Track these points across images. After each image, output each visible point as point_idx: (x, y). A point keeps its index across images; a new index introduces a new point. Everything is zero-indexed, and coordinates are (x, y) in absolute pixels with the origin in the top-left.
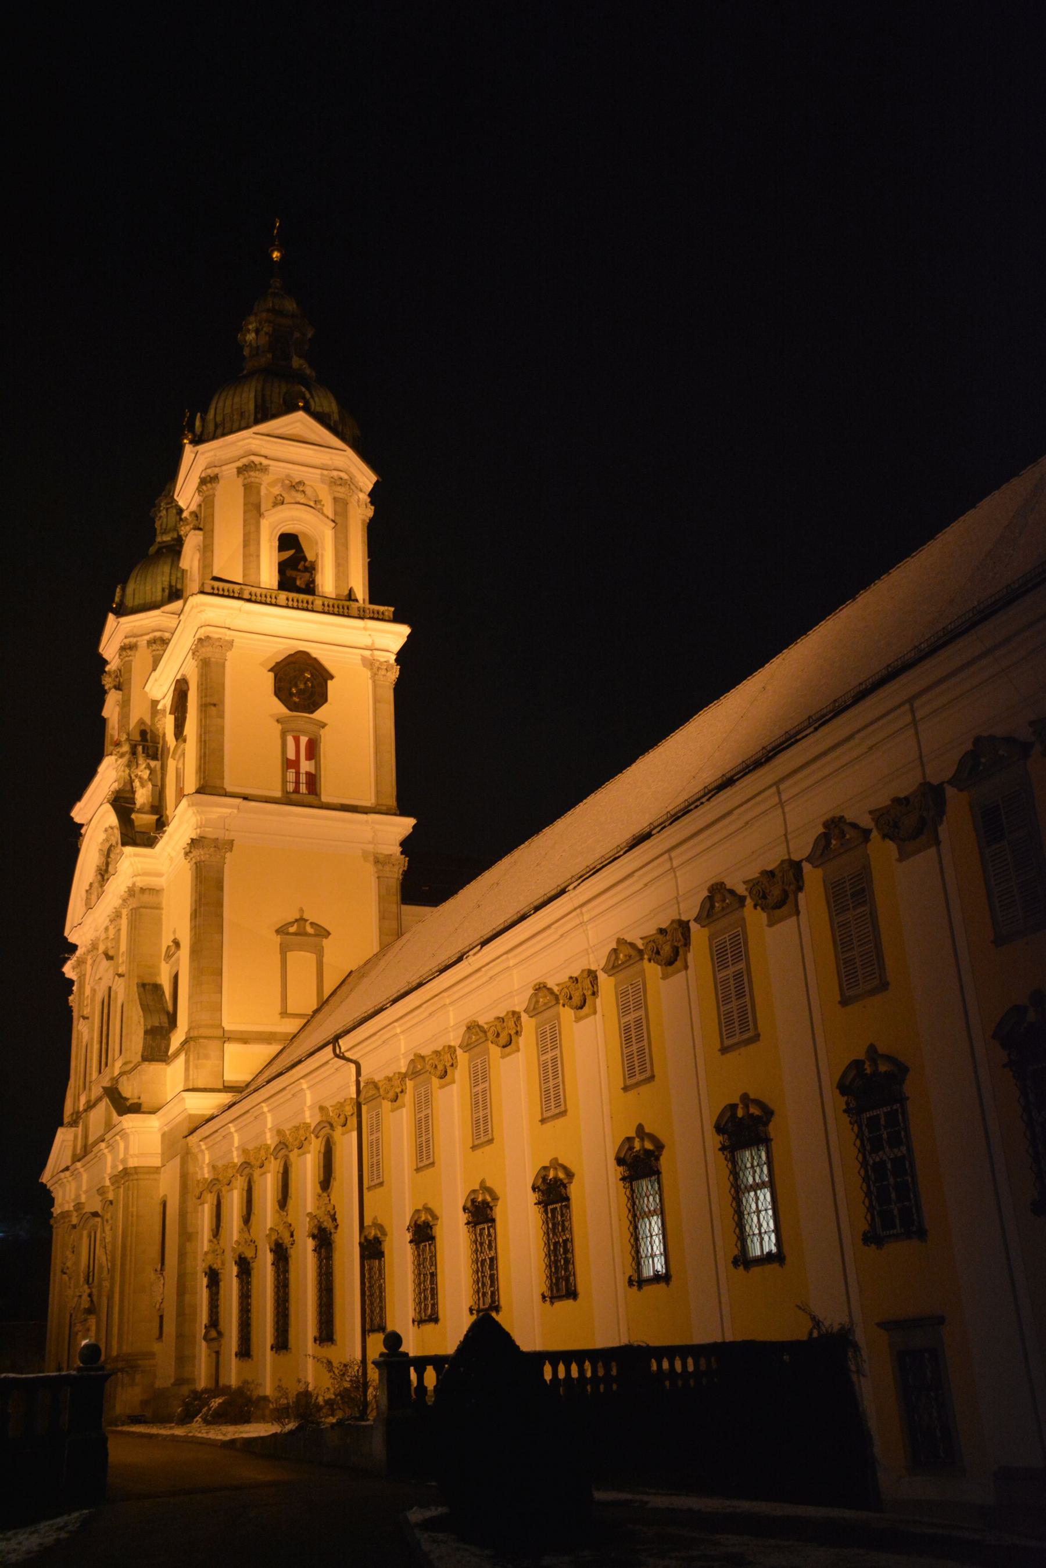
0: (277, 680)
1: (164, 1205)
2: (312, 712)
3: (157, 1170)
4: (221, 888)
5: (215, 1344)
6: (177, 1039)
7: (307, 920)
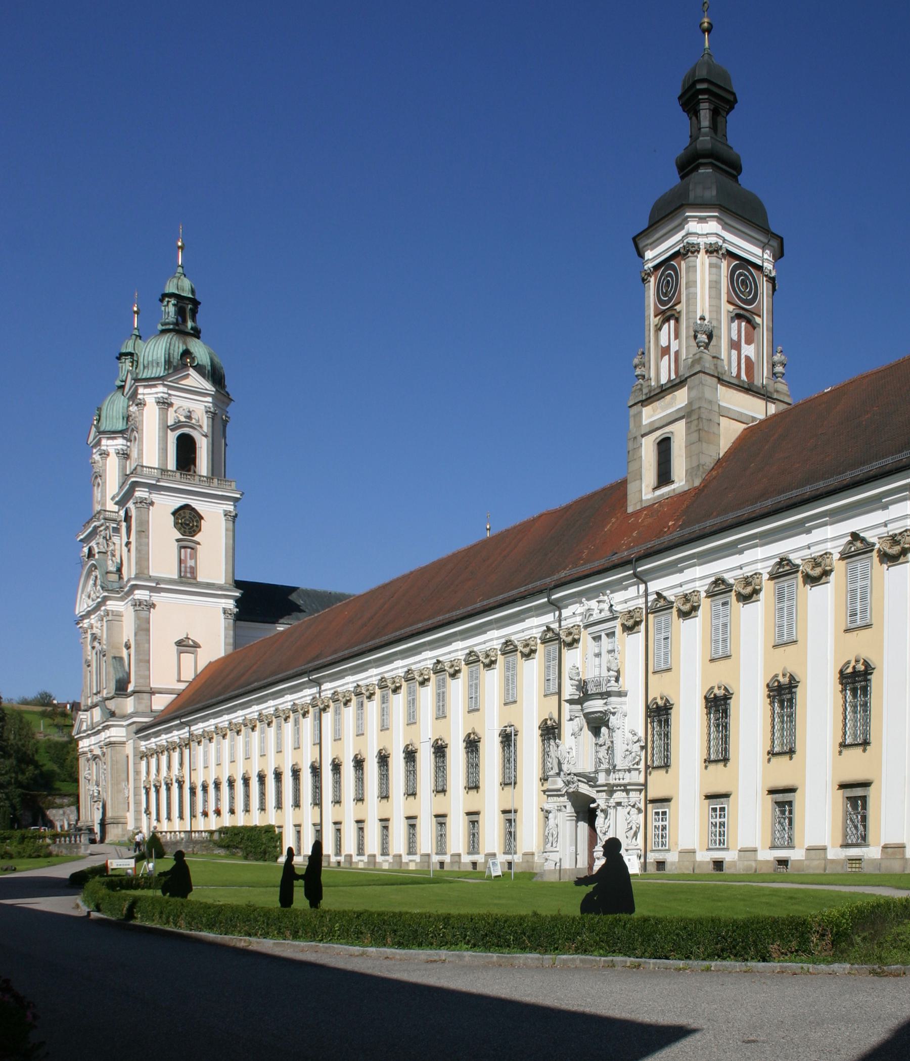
0: (176, 519)
1: (128, 757)
2: (193, 536)
3: (124, 743)
4: (149, 623)
5: (148, 816)
6: (131, 688)
7: (189, 639)
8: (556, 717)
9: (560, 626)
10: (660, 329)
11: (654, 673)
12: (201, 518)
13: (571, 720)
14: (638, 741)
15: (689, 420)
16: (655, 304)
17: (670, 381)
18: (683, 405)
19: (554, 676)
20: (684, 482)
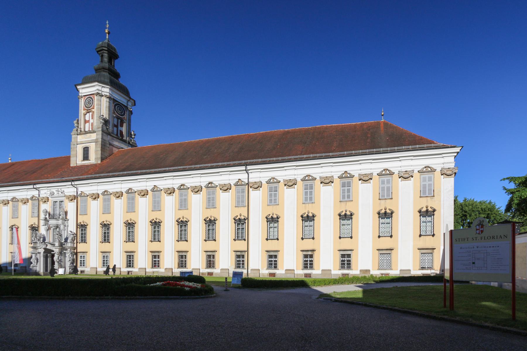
8: (37, 223)
9: (39, 196)
10: (85, 115)
11: (80, 215)
13: (43, 226)
14: (73, 235)
15: (96, 144)
16: (84, 107)
17: (89, 131)
18: (94, 139)
19: (36, 211)
20: (94, 161)
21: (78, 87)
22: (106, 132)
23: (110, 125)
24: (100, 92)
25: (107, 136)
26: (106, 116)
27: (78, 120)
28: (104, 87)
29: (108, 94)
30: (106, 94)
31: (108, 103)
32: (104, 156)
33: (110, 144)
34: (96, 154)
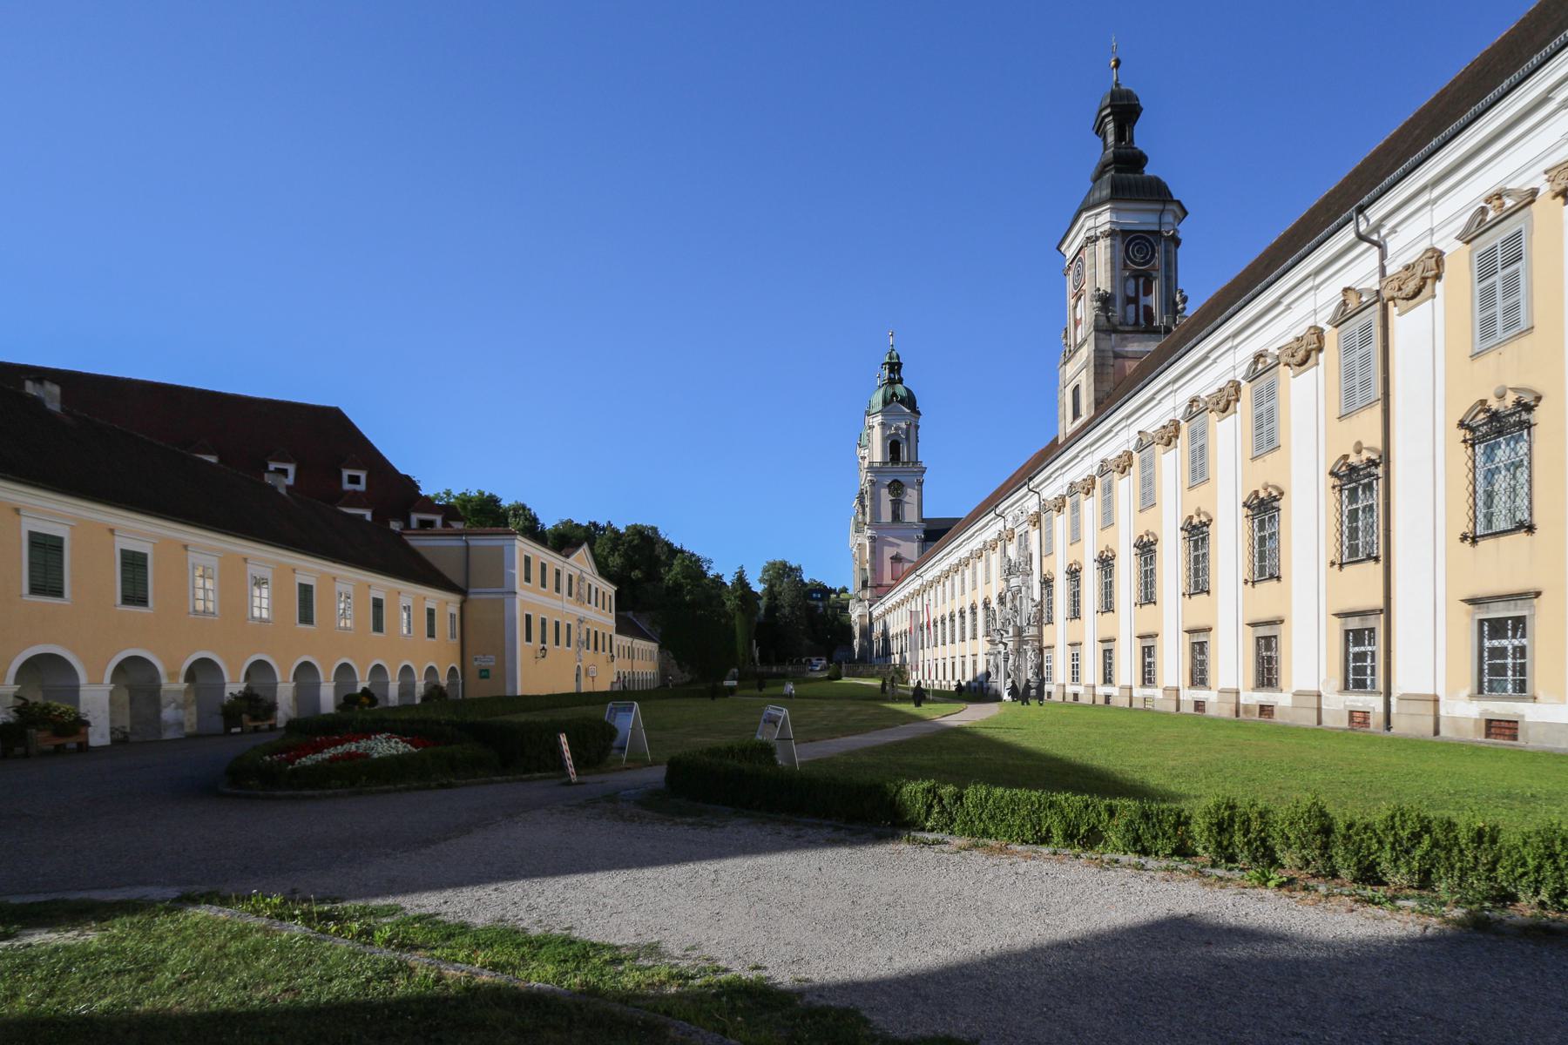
12: (903, 486)
21: (1063, 249)
22: (1104, 328)
23: (1114, 306)
24: (1092, 233)
25: (1108, 337)
26: (1104, 284)
27: (1066, 329)
28: (1099, 214)
29: (1107, 227)
30: (1102, 229)
31: (1109, 250)
32: (1101, 395)
33: (1117, 356)
34: (1088, 395)
